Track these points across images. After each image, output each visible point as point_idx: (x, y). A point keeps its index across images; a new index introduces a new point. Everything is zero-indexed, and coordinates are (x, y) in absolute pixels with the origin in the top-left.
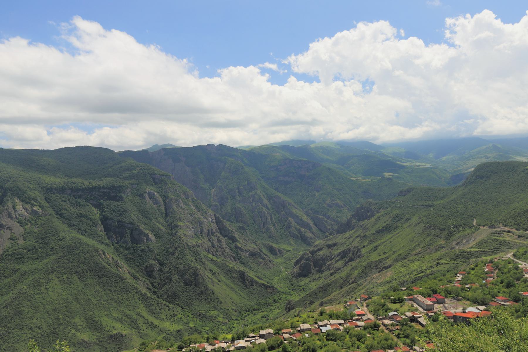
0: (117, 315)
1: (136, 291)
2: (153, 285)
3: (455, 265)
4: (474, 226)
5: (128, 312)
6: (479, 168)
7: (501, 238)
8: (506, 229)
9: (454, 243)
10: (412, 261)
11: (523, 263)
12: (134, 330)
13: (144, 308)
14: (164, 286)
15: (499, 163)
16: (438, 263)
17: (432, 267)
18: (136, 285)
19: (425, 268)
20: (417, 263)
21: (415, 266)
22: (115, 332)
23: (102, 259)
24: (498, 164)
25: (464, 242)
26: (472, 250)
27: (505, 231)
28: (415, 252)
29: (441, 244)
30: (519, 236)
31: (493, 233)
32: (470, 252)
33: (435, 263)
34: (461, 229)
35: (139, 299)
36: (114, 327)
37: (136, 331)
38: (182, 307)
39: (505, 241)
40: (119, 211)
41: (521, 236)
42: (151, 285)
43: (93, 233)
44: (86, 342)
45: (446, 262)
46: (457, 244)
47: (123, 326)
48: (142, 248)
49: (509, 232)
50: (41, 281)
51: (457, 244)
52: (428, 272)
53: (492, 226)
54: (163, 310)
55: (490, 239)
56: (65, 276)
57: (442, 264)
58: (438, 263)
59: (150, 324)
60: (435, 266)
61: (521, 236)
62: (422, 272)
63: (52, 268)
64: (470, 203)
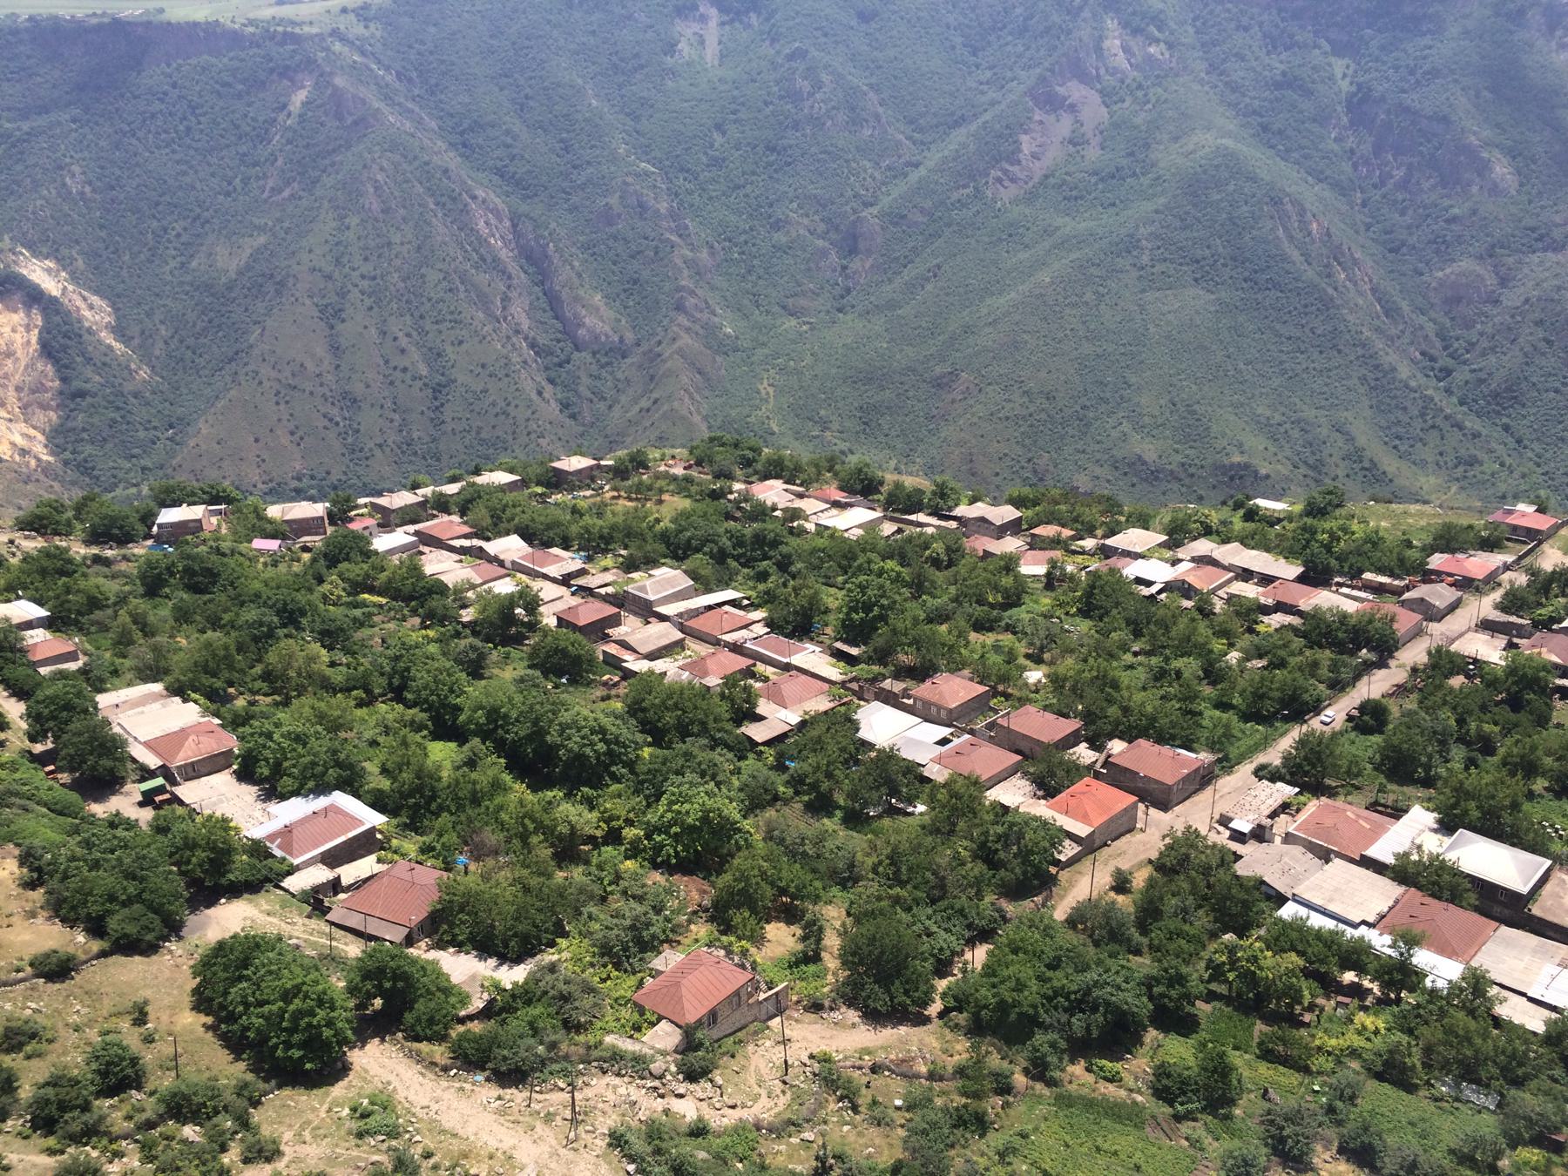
0: (1268, 413)
1: (1360, 351)
2: (1445, 348)
5: (1309, 413)
12: (1303, 470)
13: (1368, 413)
14: (1483, 354)
18: (1367, 333)
22: (1237, 459)
23: (1285, 229)
35: (1363, 379)
36: (1241, 445)
37: (1310, 473)
38: (1519, 442)
40: (1412, 73)
42: (1438, 344)
43: (1305, 142)
44: (1144, 463)
47: (1272, 449)
48: (1456, 211)
50: (1092, 270)
54: (1435, 433)
56: (1159, 268)
59: (1366, 464)
63: (1132, 236)
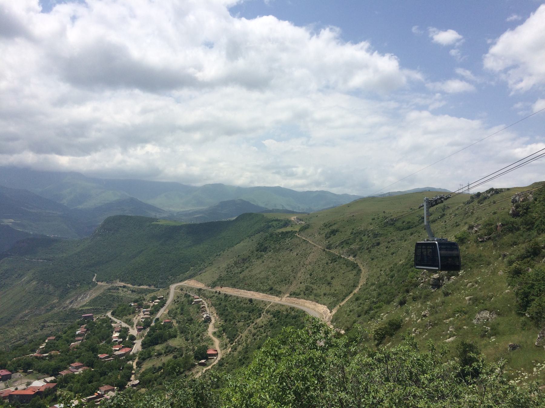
3: (62, 327)
4: (92, 281)
6: (108, 221)
7: (116, 294)
8: (122, 284)
9: (68, 302)
10: (14, 326)
11: (118, 321)
15: (128, 217)
16: (44, 326)
17: (36, 331)
19: (26, 333)
20: (19, 328)
21: (15, 332)
24: (127, 218)
25: (79, 299)
26: (84, 308)
27: (121, 287)
28: (20, 315)
29: (54, 304)
30: (133, 291)
31: (109, 289)
32: (81, 310)
33: (40, 326)
34: (78, 285)
39: (118, 297)
41: (135, 291)
45: (52, 324)
46: (71, 303)
49: (124, 287)
51: (71, 303)
52: (29, 338)
53: (109, 281)
55: (105, 296)
57: (48, 326)
58: (44, 326)
60: (39, 330)
61: (135, 291)
62: (23, 338)
64: (94, 257)
